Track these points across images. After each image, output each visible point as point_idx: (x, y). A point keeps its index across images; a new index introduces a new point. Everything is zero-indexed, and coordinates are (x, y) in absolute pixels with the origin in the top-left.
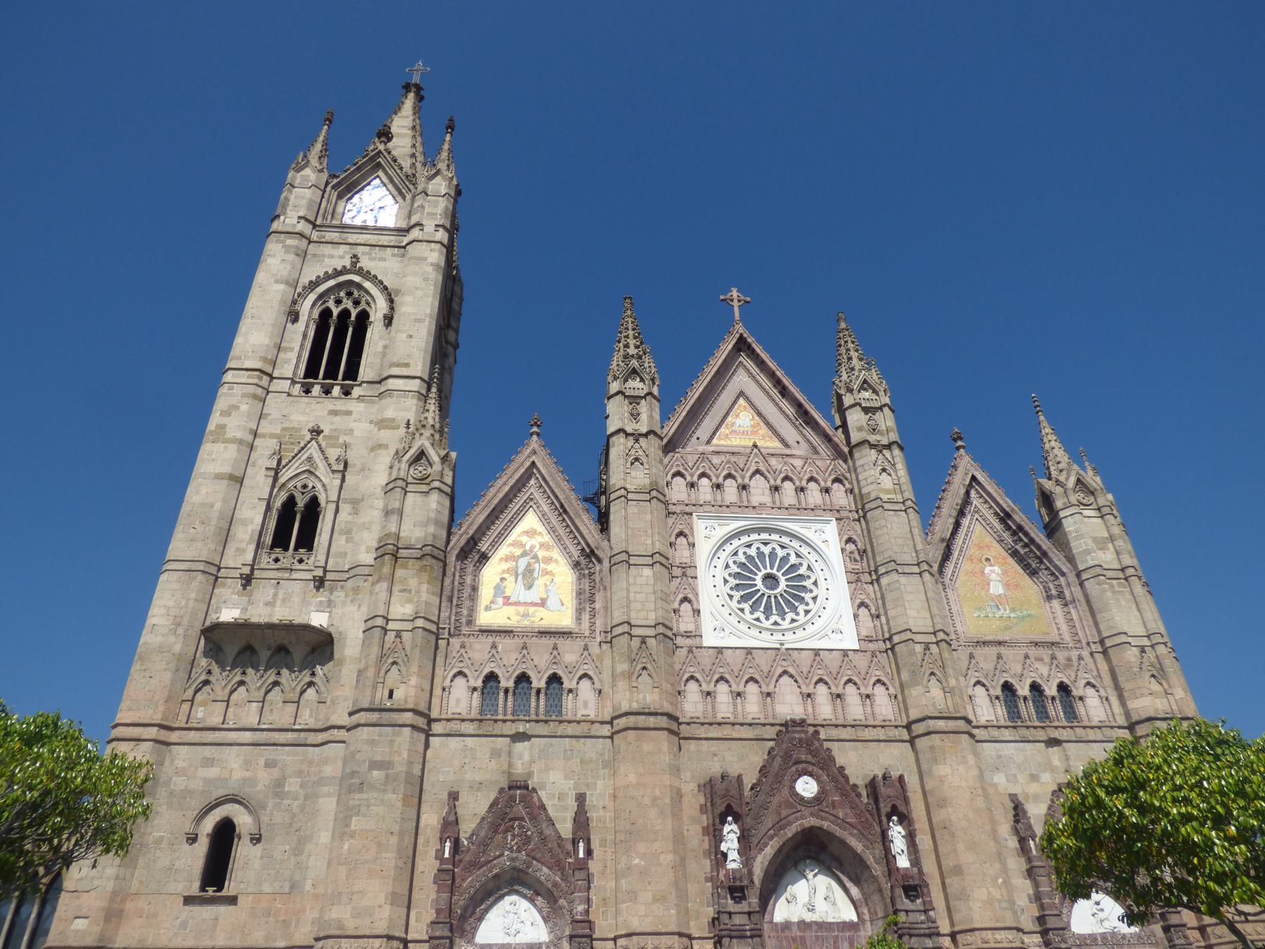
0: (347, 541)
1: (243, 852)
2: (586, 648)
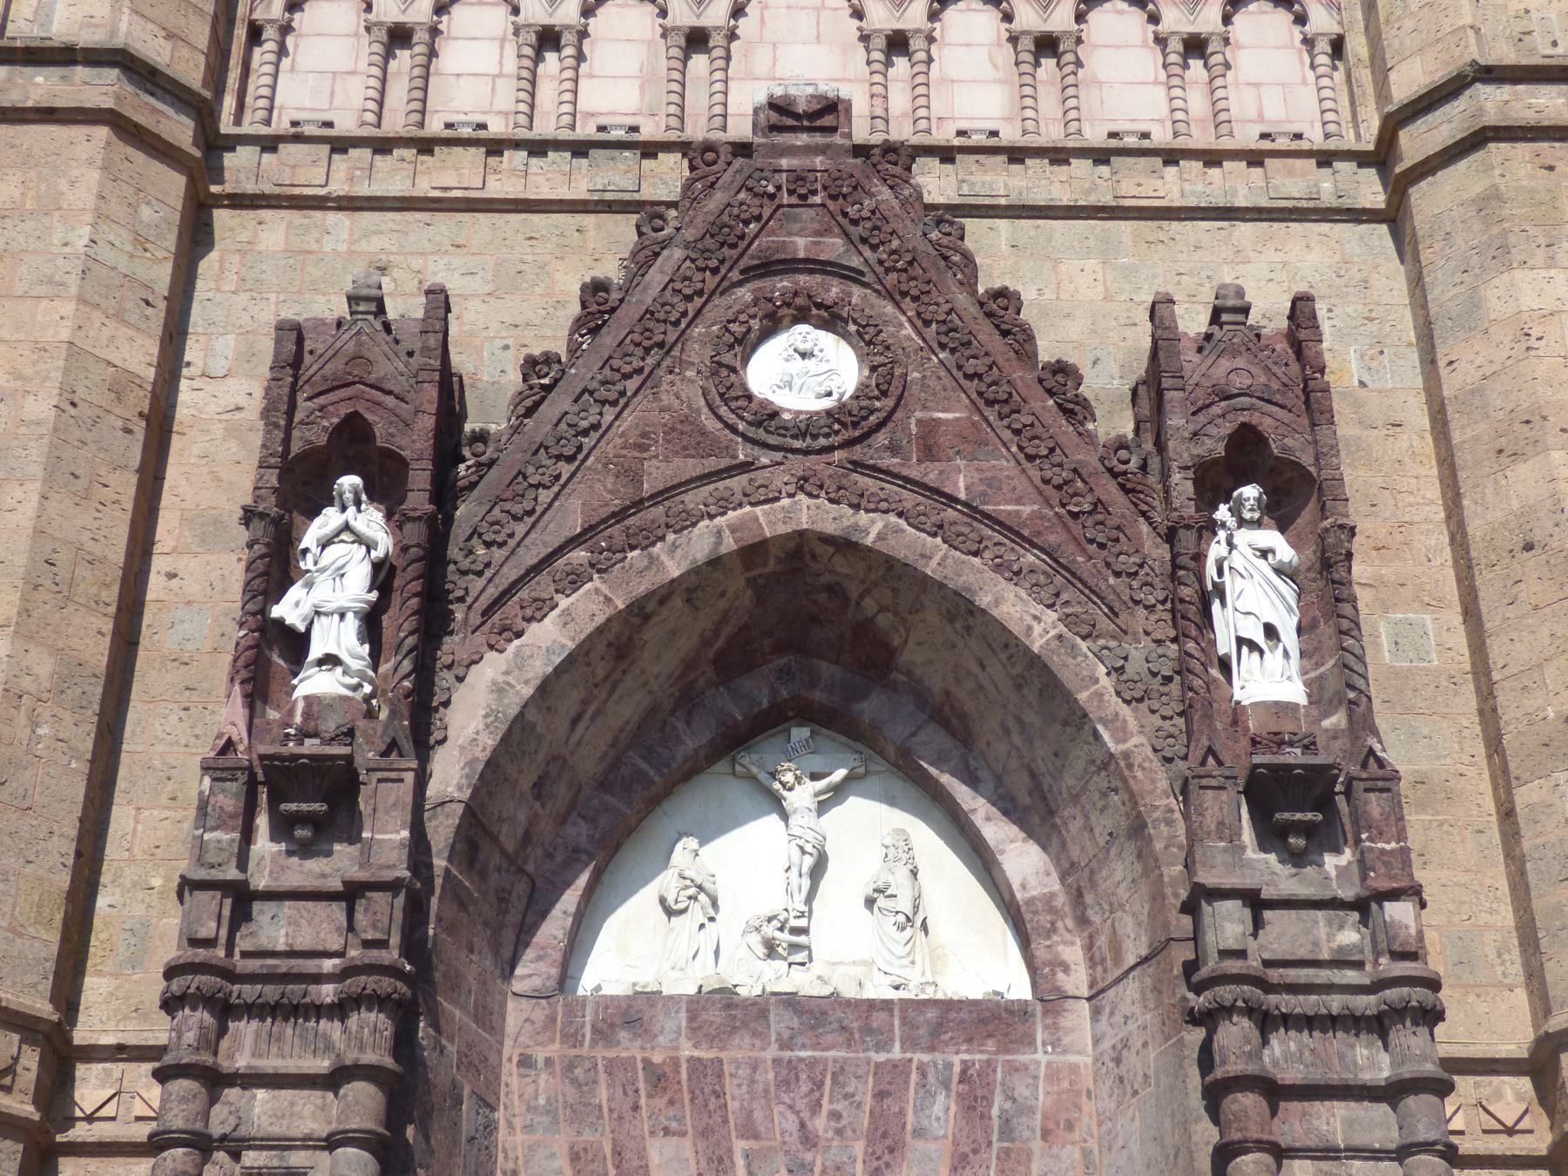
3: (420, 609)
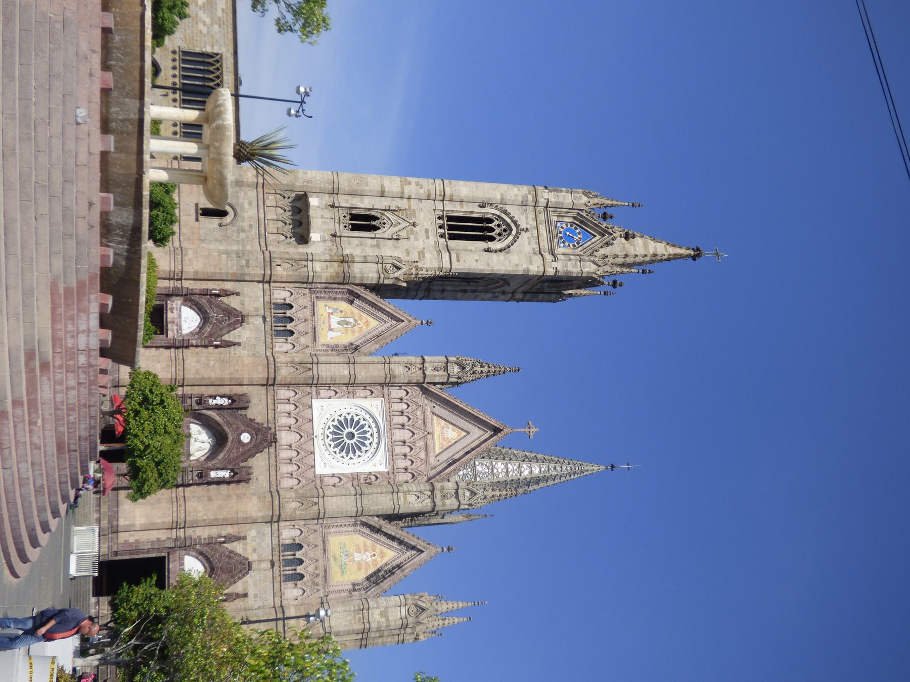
0: (357, 245)
1: (215, 221)
2: (307, 347)
3: (219, 408)
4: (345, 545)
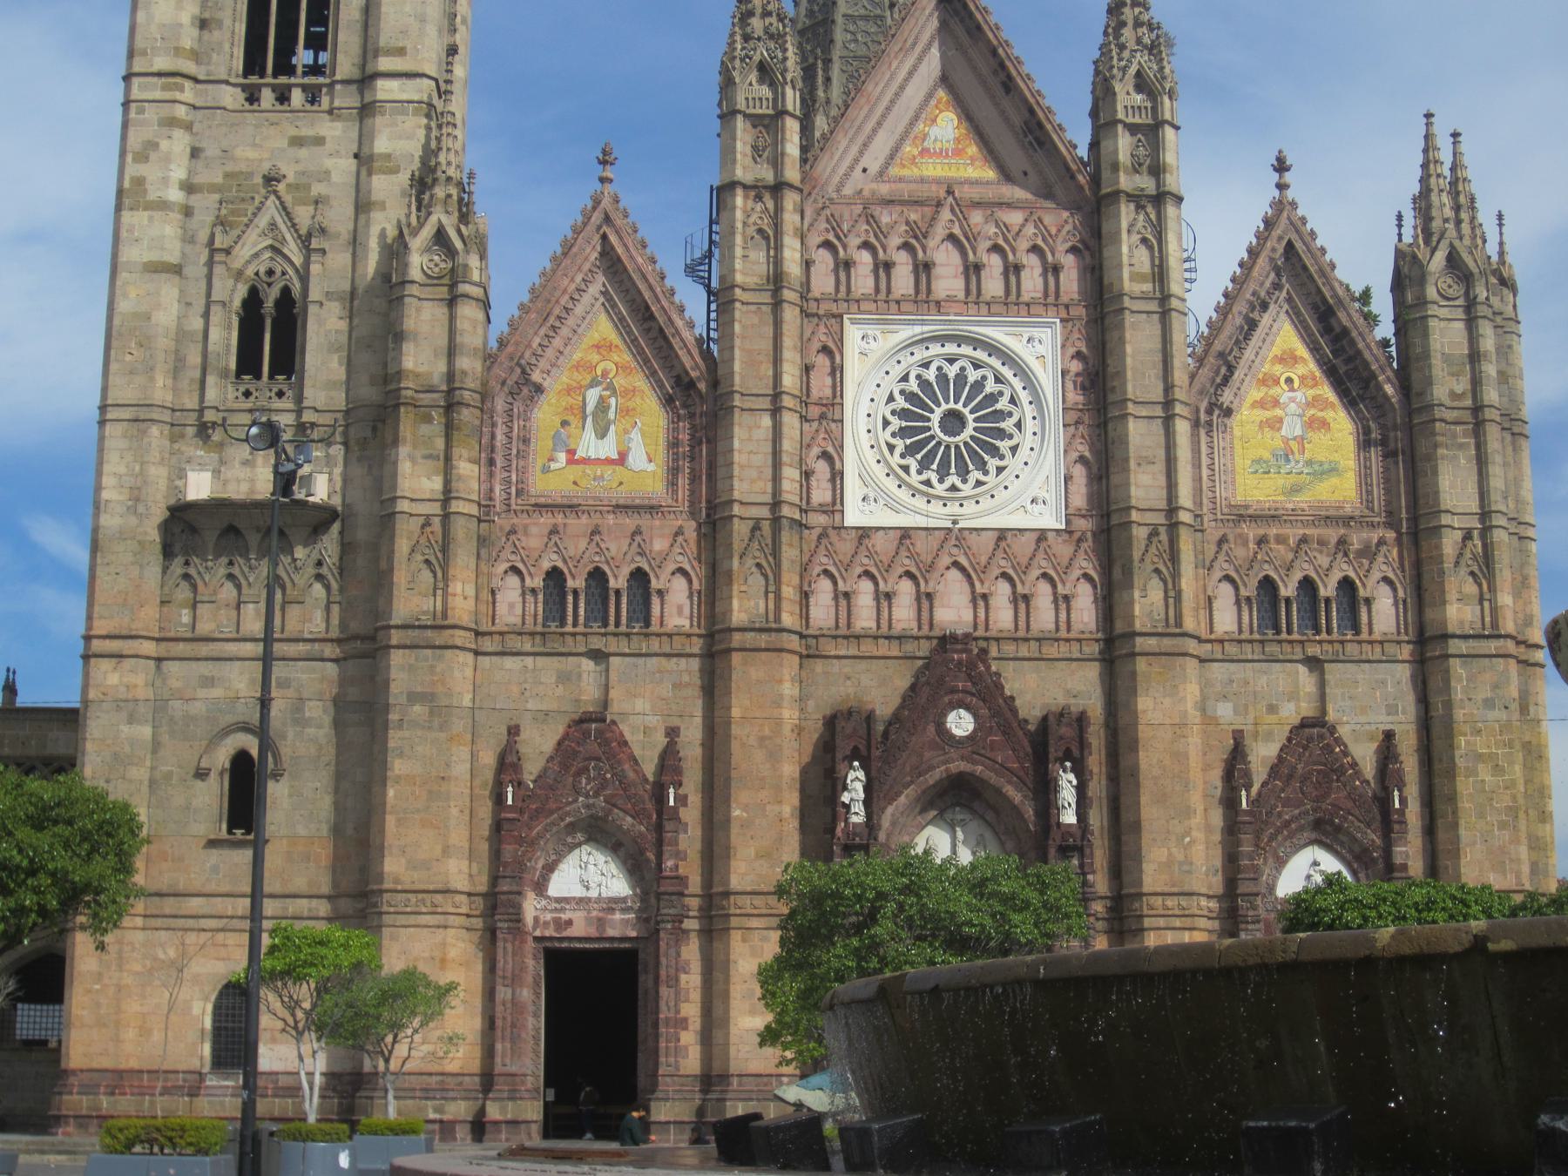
4: (1258, 461)
